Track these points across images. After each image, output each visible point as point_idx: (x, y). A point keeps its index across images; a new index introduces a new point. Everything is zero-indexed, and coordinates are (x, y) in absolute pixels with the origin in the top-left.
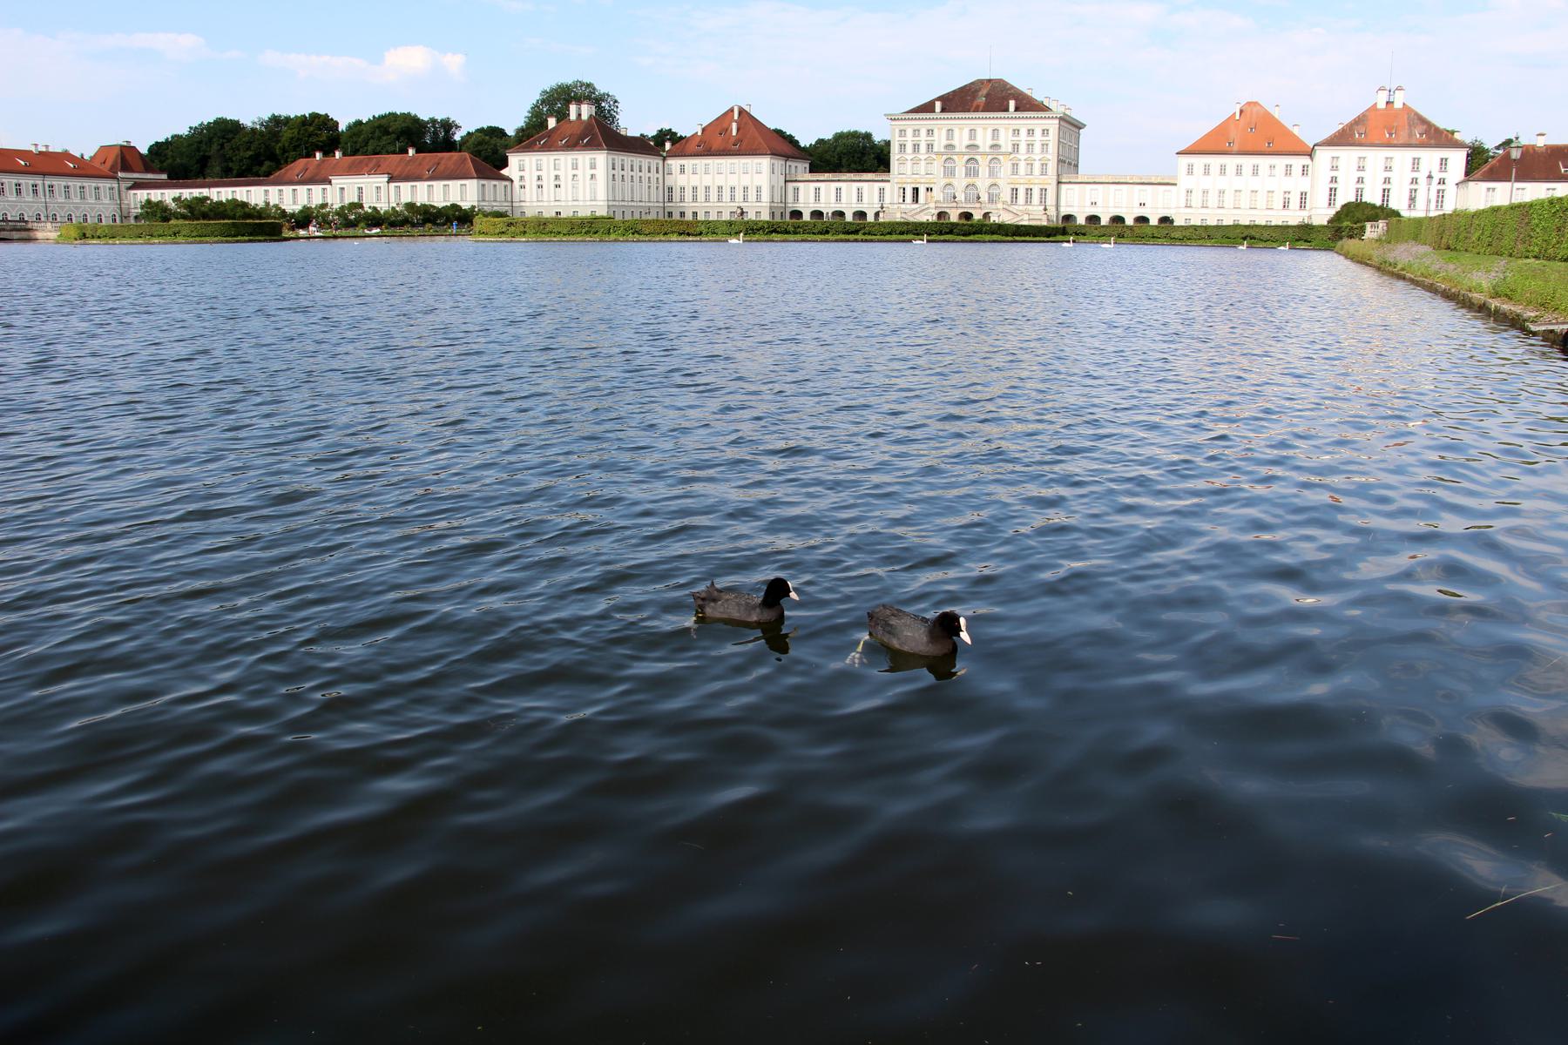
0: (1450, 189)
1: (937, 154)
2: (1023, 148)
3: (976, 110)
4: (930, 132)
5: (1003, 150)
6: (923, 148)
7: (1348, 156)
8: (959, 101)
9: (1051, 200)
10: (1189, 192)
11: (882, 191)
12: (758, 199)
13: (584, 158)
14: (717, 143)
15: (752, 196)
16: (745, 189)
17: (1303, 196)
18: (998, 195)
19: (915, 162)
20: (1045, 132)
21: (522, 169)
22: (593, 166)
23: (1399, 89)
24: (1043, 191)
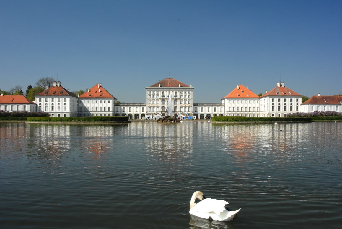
0: (299, 106)
2: (183, 97)
4: (157, 92)
5: (178, 97)
6: (156, 96)
7: (276, 99)
8: (164, 85)
9: (191, 110)
10: (230, 108)
11: (143, 108)
12: (109, 111)
13: (62, 99)
14: (95, 95)
15: (107, 110)
16: (105, 108)
19: (154, 100)
21: (40, 101)
22: (65, 101)
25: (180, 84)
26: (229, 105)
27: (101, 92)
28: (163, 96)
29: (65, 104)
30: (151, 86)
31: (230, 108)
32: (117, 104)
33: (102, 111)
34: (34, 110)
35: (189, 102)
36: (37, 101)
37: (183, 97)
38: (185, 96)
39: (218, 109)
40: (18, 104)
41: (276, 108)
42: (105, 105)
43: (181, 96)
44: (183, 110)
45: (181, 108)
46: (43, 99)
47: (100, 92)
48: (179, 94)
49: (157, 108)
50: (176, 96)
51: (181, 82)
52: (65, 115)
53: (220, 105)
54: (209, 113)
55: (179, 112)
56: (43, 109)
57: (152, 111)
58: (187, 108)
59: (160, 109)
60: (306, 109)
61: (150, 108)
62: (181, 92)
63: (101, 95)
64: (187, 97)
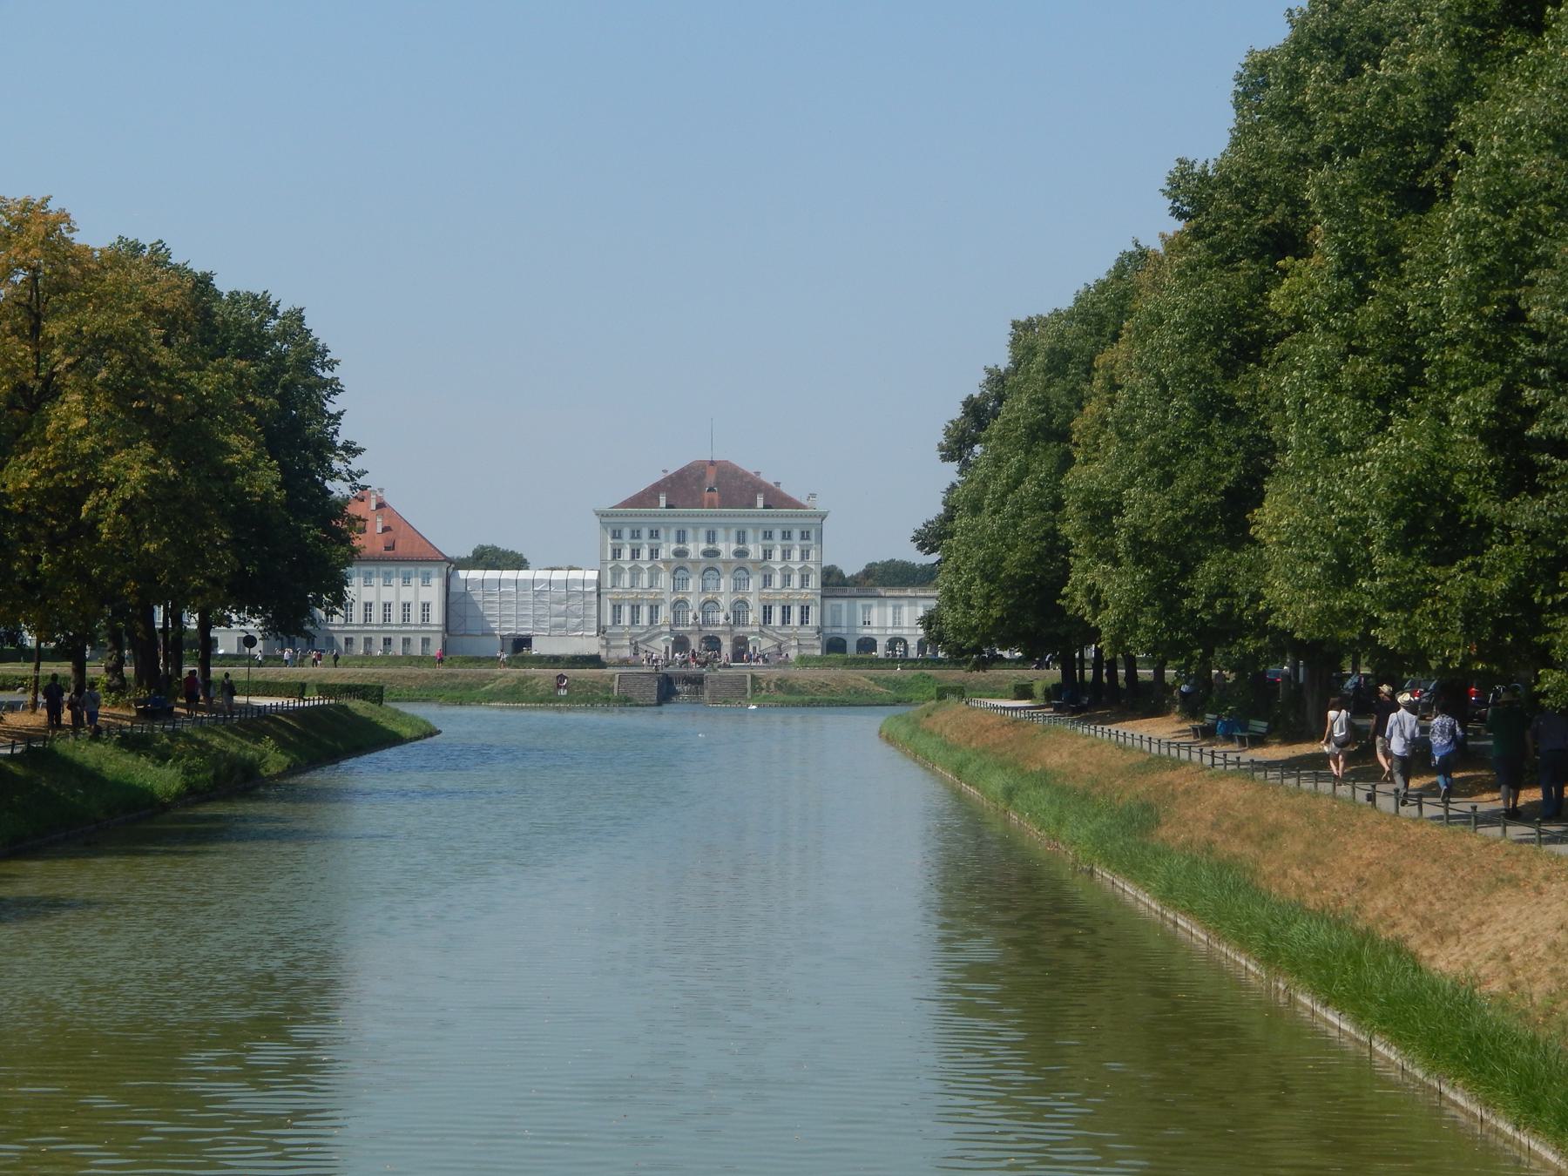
1: (665, 562)
2: (777, 555)
3: (711, 506)
15: (415, 615)
16: (406, 606)
19: (636, 572)
20: (805, 536)
24: (805, 611)
25: (760, 491)
27: (385, 529)
30: (625, 504)
33: (393, 621)
37: (777, 555)
38: (786, 554)
43: (767, 554)
45: (767, 613)
47: (380, 530)
49: (654, 610)
51: (768, 478)
54: (897, 632)
55: (757, 629)
59: (665, 614)
61: (617, 609)
63: (387, 549)
64: (796, 555)
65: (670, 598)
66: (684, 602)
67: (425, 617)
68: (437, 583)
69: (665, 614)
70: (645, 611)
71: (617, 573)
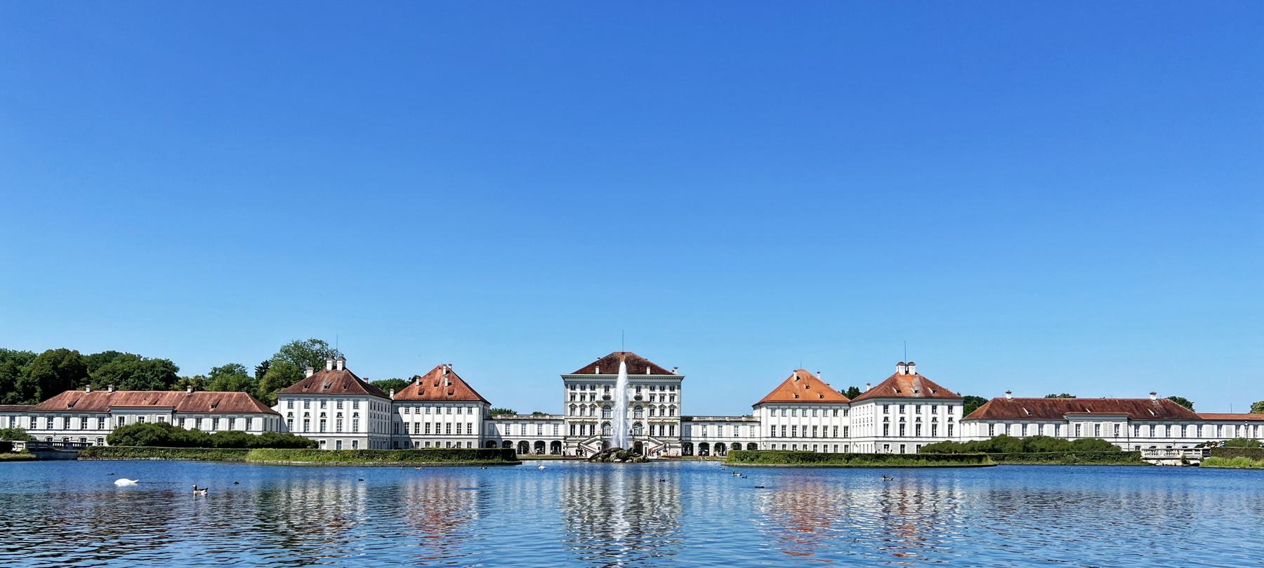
2: (657, 399)
6: (588, 398)
9: (677, 432)
10: (773, 427)
14: (435, 393)
15: (464, 430)
17: (846, 428)
18: (641, 431)
19: (583, 408)
21: (290, 406)
23: (912, 364)
26: (773, 421)
28: (607, 398)
29: (356, 414)
31: (773, 427)
32: (488, 416)
34: (274, 429)
35: (672, 411)
36: (282, 407)
37: (657, 399)
38: (662, 398)
39: (744, 431)
40: (233, 413)
41: (894, 430)
42: (459, 418)
43: (652, 398)
44: (657, 433)
45: (652, 427)
46: (299, 405)
48: (645, 393)
49: (592, 427)
50: (638, 398)
52: (355, 443)
53: (750, 421)
54: (720, 440)
56: (297, 428)
57: (578, 432)
58: (667, 428)
60: (973, 432)
61: (573, 427)
62: (653, 389)
64: (667, 399)
65: (600, 421)
66: (608, 424)
67: (469, 432)
68: (475, 410)
69: (598, 429)
70: (588, 427)
71: (573, 408)
